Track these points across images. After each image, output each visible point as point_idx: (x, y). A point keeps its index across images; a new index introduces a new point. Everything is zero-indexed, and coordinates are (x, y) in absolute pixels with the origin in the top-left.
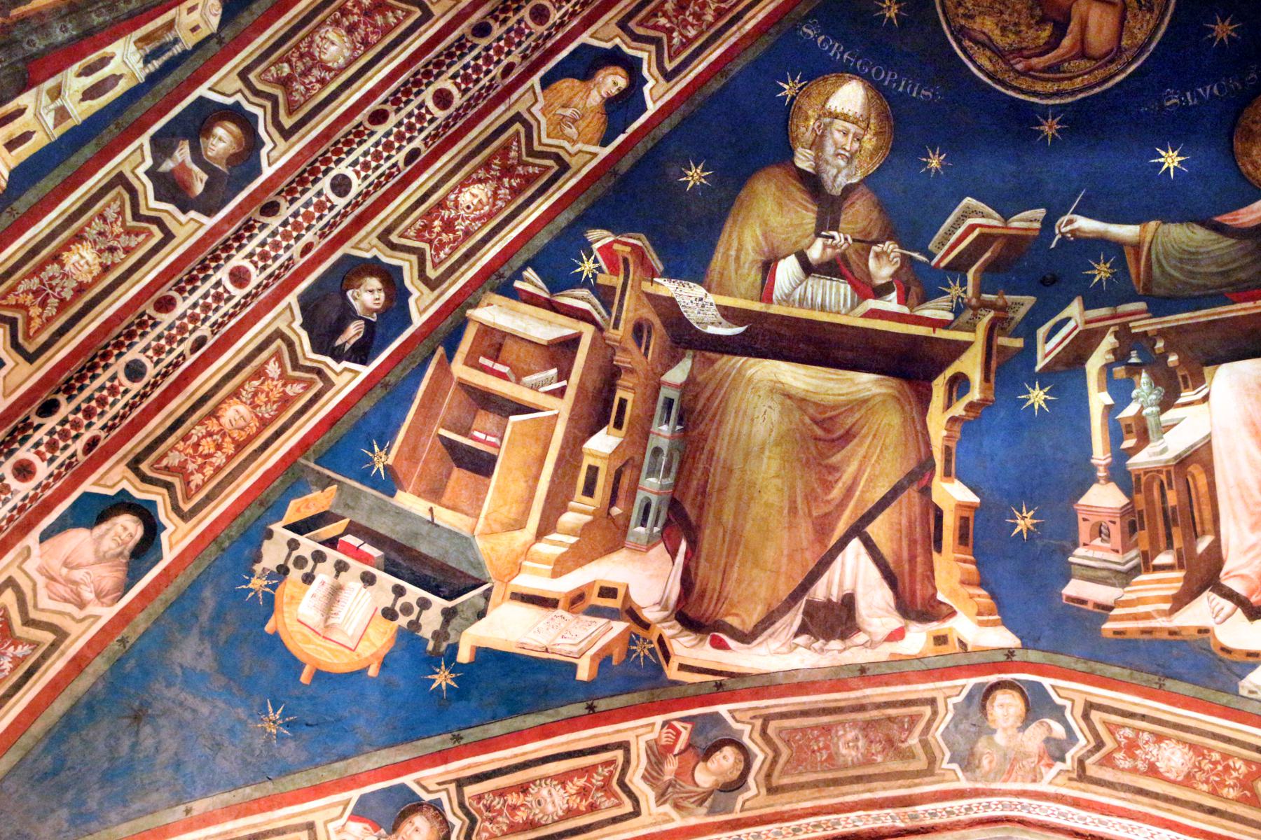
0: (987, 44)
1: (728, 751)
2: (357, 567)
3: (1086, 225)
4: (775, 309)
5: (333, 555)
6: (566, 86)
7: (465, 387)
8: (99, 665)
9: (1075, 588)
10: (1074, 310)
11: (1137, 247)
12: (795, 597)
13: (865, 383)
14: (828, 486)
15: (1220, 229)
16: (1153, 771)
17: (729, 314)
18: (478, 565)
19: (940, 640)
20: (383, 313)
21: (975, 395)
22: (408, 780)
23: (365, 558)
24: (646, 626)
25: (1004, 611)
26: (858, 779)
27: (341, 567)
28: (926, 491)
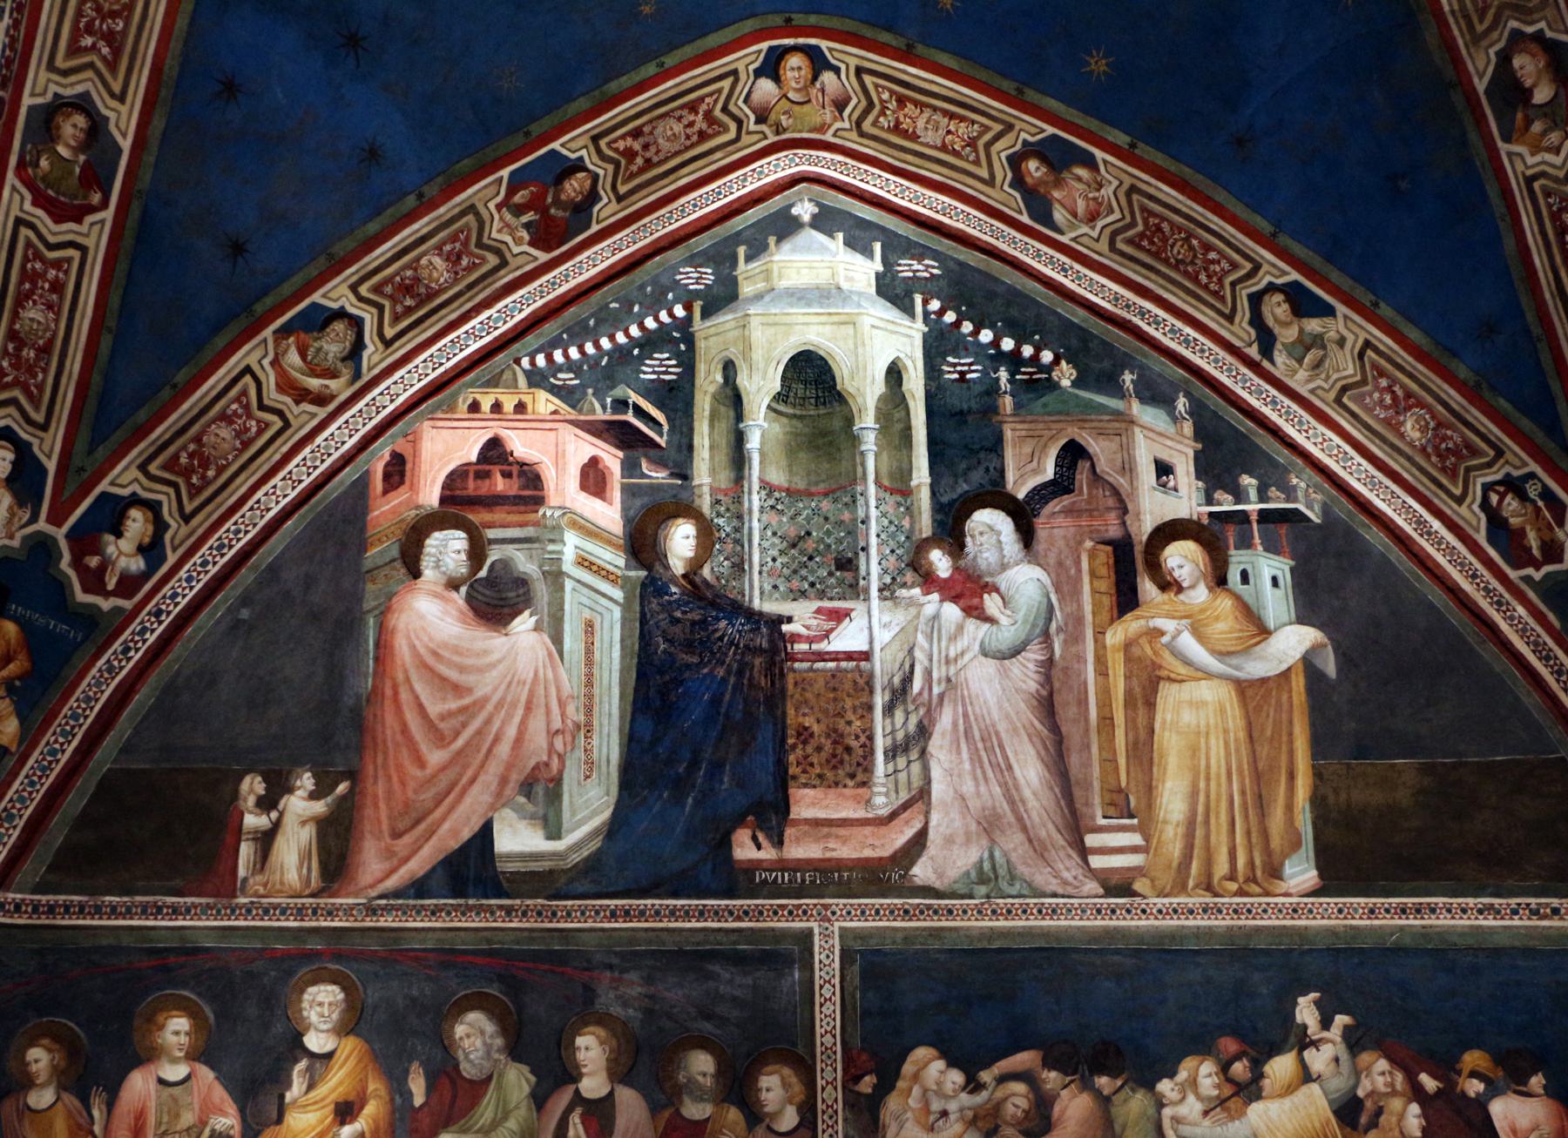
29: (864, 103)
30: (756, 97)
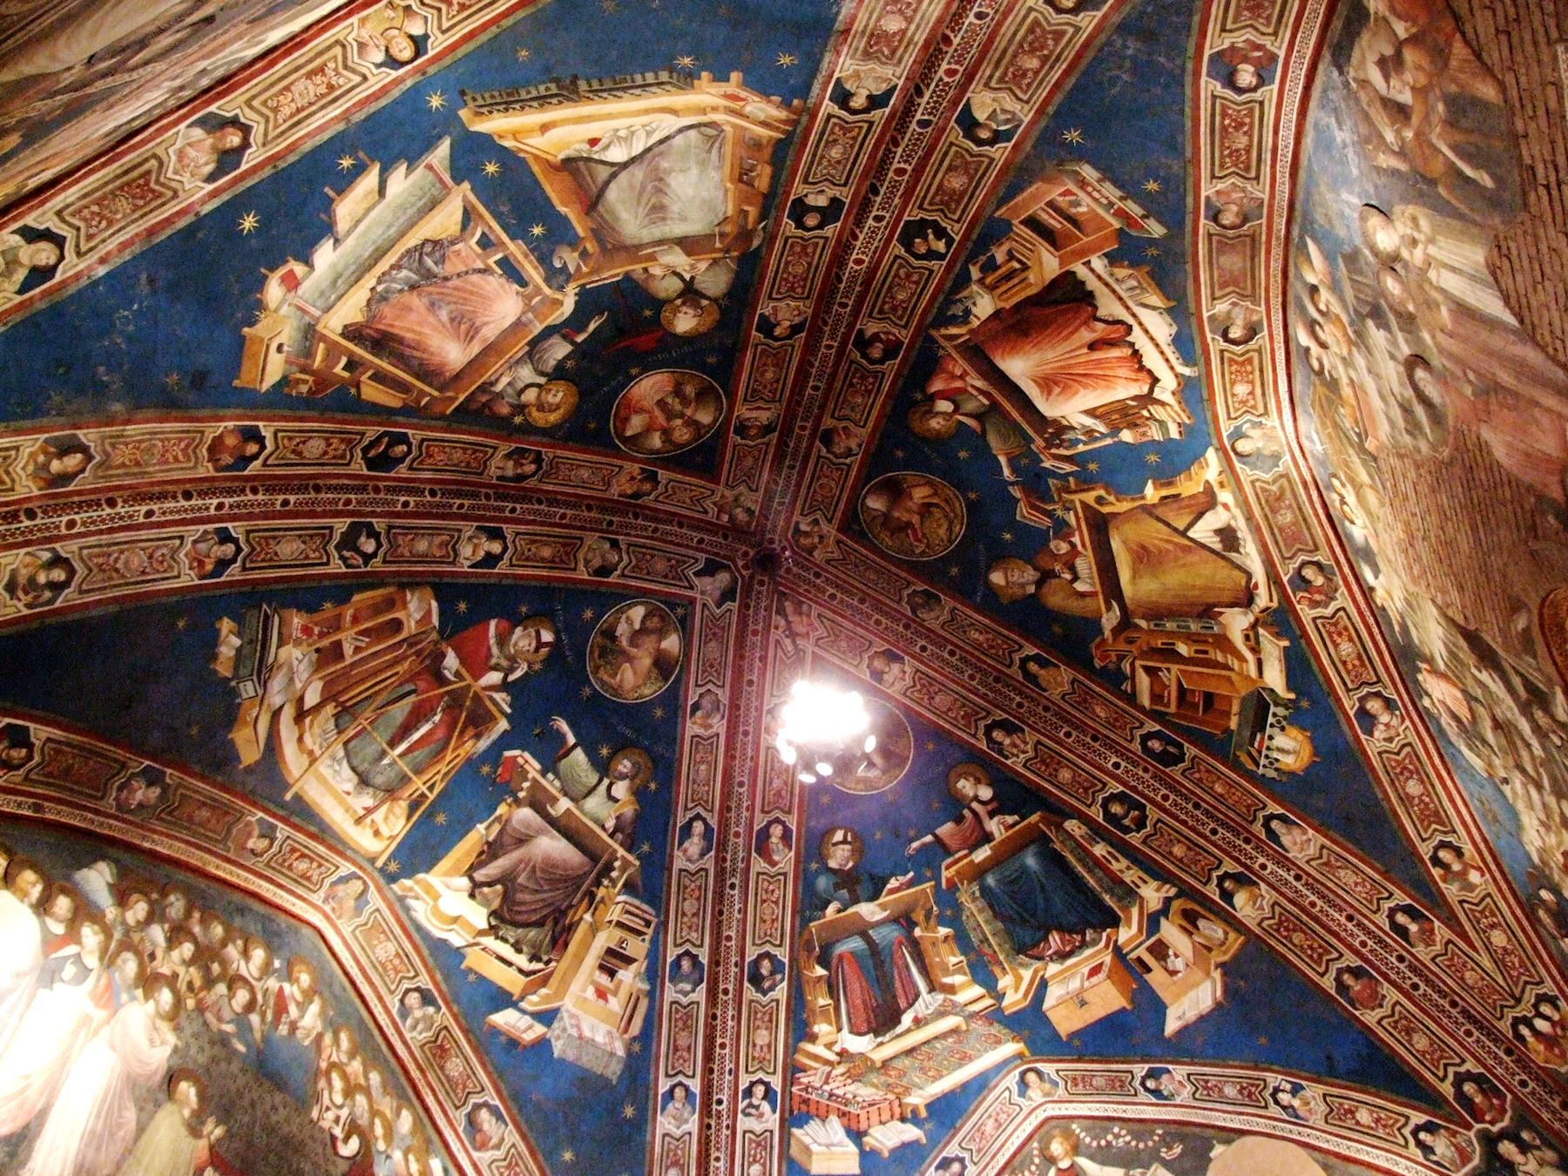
0: (950, 529)
1: (1304, 573)
2: (1266, 742)
3: (1006, 472)
4: (1098, 588)
5: (1264, 752)
6: (1044, 684)
7: (1179, 706)
8: (1331, 833)
9: (1174, 433)
10: (1047, 464)
11: (1006, 454)
12: (1223, 557)
13: (1116, 544)
14: (1168, 551)
15: (984, 431)
16: (1252, 393)
17: (1109, 608)
18: (1252, 694)
19: (1222, 485)
20: (1160, 740)
21: (1102, 492)
22: (1351, 713)
23: (1262, 739)
24: (1257, 620)
25: (1197, 456)
26: (1300, 509)
27: (1268, 748)
28: (1154, 505)
29: (350, 63)
30: (420, 22)
